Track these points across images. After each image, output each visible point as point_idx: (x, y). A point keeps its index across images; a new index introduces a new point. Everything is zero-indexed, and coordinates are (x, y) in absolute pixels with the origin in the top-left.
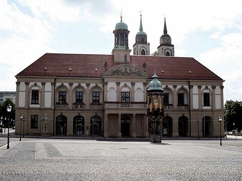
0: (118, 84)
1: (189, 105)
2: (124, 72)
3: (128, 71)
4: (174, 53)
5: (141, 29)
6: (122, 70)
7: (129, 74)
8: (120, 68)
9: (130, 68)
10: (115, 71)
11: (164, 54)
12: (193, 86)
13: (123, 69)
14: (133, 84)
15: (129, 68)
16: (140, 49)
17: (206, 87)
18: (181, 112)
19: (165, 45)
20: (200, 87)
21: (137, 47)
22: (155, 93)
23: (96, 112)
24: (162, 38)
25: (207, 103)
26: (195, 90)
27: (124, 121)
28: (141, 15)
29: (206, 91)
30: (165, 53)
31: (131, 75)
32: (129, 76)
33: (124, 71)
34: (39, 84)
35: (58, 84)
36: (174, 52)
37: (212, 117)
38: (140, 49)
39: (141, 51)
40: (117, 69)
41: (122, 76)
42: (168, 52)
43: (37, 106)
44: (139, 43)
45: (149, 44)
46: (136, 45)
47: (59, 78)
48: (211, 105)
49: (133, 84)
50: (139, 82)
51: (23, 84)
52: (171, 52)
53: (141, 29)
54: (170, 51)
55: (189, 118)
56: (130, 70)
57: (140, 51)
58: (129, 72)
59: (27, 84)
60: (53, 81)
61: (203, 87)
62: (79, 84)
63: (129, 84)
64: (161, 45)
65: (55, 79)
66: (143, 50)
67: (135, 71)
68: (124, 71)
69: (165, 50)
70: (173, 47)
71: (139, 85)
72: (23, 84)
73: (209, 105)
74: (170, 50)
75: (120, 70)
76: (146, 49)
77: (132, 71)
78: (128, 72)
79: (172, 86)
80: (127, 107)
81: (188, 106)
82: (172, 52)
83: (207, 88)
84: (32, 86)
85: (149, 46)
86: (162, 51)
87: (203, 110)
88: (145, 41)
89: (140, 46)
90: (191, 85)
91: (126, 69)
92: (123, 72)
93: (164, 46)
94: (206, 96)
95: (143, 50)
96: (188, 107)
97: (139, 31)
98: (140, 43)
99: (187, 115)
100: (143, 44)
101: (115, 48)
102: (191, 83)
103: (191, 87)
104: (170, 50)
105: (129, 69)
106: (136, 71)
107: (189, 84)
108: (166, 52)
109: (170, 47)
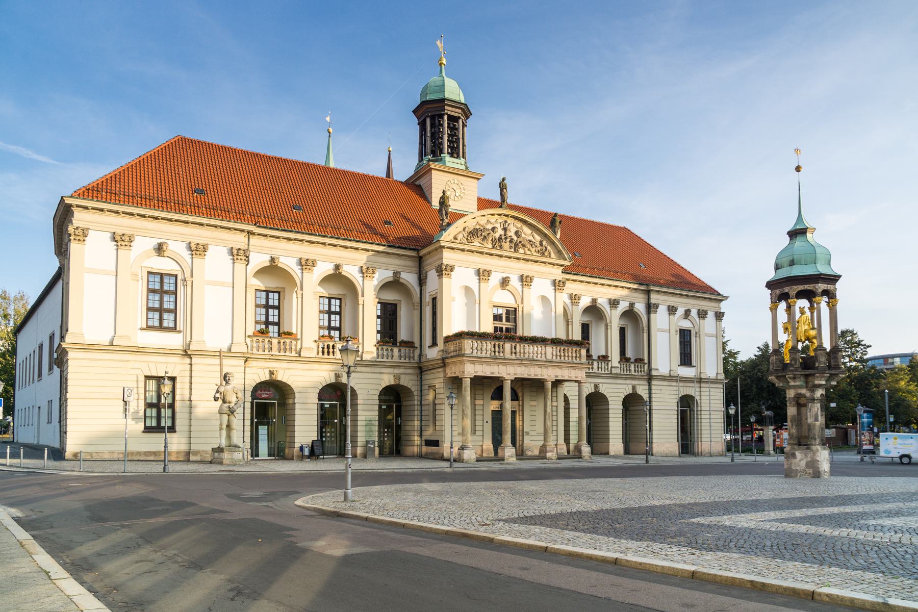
0: (484, 275)
1: (646, 361)
13: (498, 226)
18: (628, 382)
23: (397, 371)
31: (521, 251)
32: (516, 251)
33: (500, 232)
34: (177, 248)
37: (697, 398)
40: (482, 223)
43: (174, 341)
48: (694, 363)
49: (525, 280)
68: (500, 232)
71: (542, 286)
75: (489, 227)
92: (497, 235)
94: (685, 337)
99: (642, 391)
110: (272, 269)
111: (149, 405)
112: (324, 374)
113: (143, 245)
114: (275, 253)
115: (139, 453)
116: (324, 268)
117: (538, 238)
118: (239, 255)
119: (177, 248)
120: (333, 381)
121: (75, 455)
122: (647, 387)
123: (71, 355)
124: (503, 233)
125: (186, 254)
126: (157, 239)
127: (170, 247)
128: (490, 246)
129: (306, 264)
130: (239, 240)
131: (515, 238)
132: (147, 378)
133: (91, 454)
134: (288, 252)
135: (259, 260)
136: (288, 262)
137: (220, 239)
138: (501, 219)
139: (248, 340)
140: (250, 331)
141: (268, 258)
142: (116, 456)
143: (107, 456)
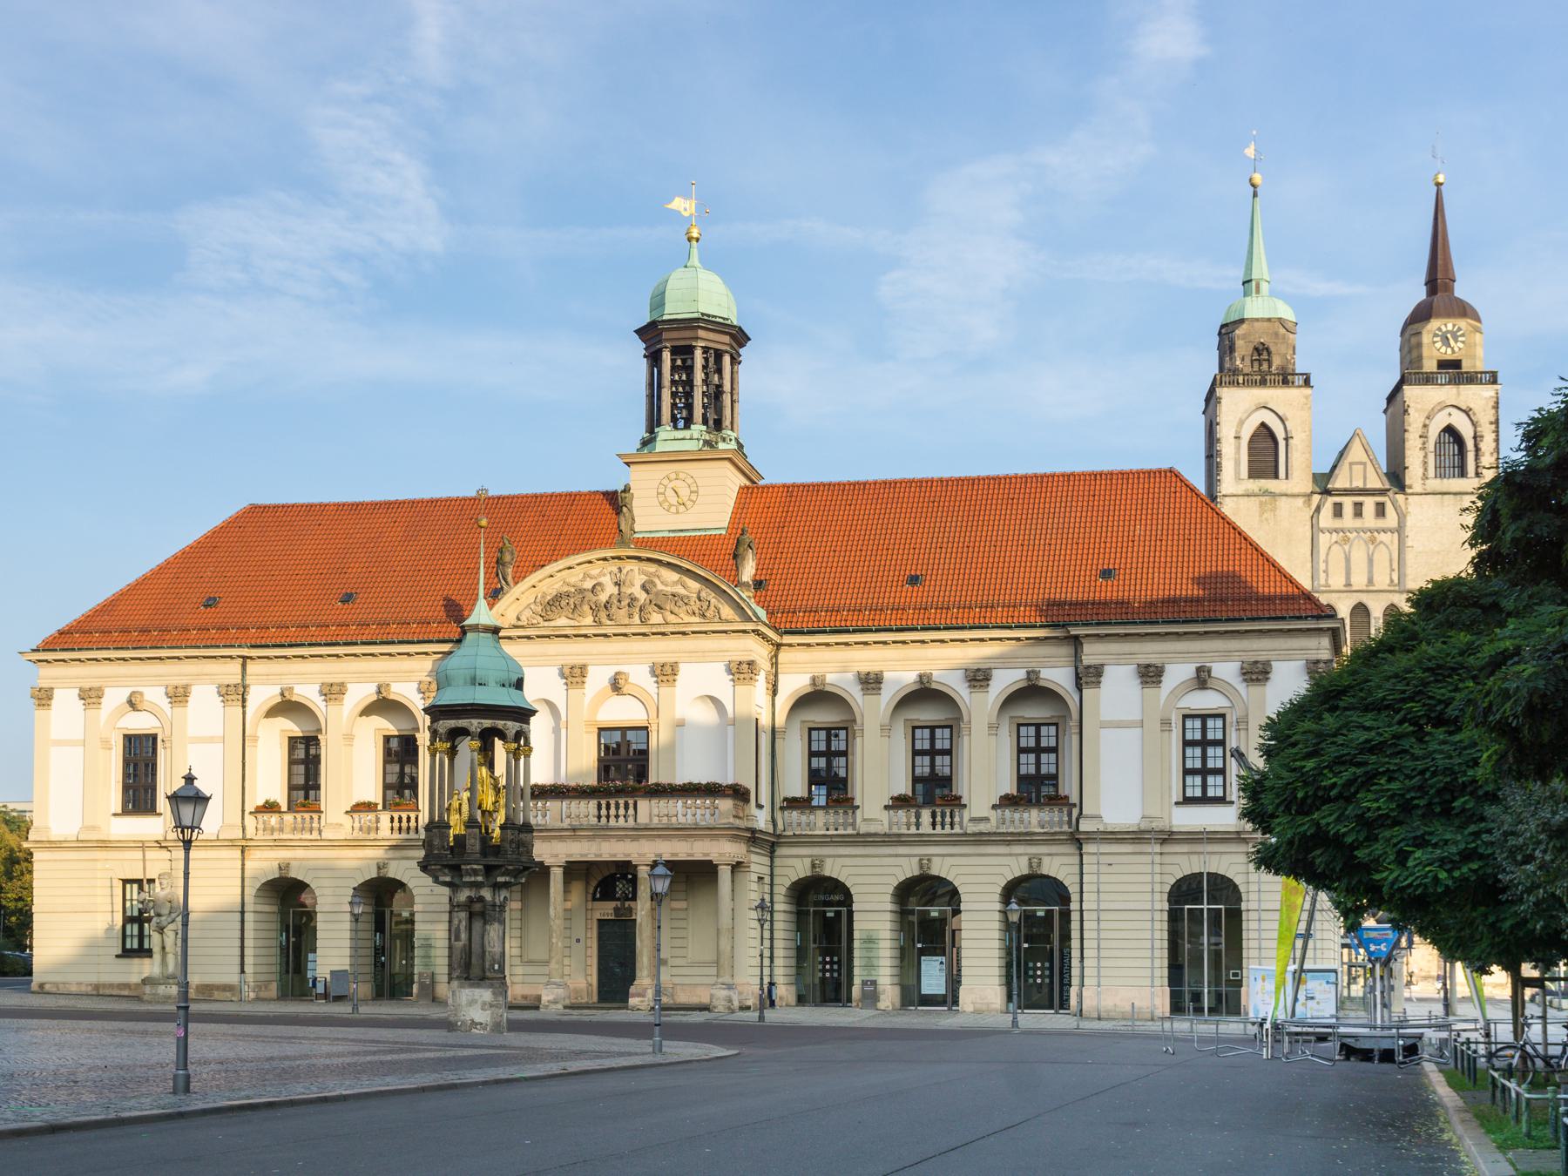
4: (1497, 432)
8: (586, 576)
10: (558, 598)
15: (642, 572)
16: (1241, 423)
17: (1199, 670)
27: (616, 909)
34: (155, 695)
38: (1241, 423)
39: (1246, 434)
40: (573, 580)
41: (599, 624)
42: (1450, 430)
47: (790, 645)
49: (665, 673)
50: (702, 657)
54: (1463, 415)
55: (1073, 890)
63: (639, 675)
66: (1263, 425)
72: (66, 700)
75: (588, 585)
83: (1202, 679)
87: (1168, 837)
92: (603, 598)
95: (1263, 425)
96: (1070, 815)
103: (1087, 677)
110: (287, 707)
111: (128, 920)
112: (361, 862)
113: (115, 697)
114: (287, 681)
115: (111, 986)
116: (361, 693)
117: (694, 585)
118: (237, 693)
119: (1226, 671)
120: (374, 875)
121: (41, 986)
122: (1076, 859)
123: (37, 856)
124: (615, 590)
125: (164, 703)
126: (135, 690)
127: (146, 697)
128: (589, 620)
129: (333, 692)
130: (230, 672)
131: (642, 597)
132: (125, 882)
133: (56, 984)
134: (304, 677)
135: (262, 695)
136: (308, 693)
137: (205, 677)
138: (613, 567)
139: (250, 820)
140: (249, 807)
141: (373, 688)
142: (83, 989)
143: (74, 989)
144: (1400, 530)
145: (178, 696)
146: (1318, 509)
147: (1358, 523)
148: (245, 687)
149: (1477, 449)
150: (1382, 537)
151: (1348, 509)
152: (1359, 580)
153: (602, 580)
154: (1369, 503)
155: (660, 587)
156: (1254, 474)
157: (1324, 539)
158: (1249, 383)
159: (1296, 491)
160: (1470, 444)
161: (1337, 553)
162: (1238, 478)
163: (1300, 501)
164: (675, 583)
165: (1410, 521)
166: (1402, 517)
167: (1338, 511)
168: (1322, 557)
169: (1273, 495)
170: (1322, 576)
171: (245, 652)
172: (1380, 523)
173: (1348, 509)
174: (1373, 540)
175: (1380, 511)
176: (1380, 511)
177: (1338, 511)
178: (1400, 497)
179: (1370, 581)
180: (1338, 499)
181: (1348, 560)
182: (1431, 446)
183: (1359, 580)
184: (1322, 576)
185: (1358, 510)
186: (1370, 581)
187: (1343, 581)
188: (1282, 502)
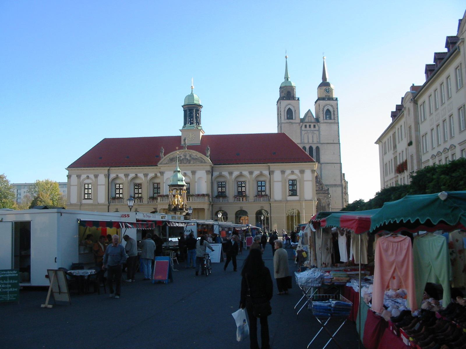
2: (183, 159)
3: (188, 157)
4: (338, 110)
5: (287, 78)
6: (180, 156)
7: (189, 161)
9: (190, 153)
11: (322, 112)
12: (273, 172)
14: (194, 173)
16: (285, 107)
19: (323, 99)
20: (283, 172)
21: (280, 106)
22: (174, 188)
24: (319, 89)
25: (293, 193)
26: (277, 176)
28: (286, 58)
29: (293, 177)
30: (323, 111)
32: (189, 163)
35: (112, 176)
36: (337, 108)
38: (285, 107)
44: (284, 100)
45: (298, 99)
46: (279, 103)
49: (194, 173)
51: (74, 178)
52: (334, 108)
53: (287, 78)
54: (331, 107)
56: (190, 156)
57: (284, 111)
58: (189, 158)
59: (79, 176)
60: (106, 172)
61: (288, 172)
62: (136, 175)
64: (319, 99)
65: (109, 169)
67: (197, 158)
68: (183, 157)
69: (324, 107)
70: (336, 102)
73: (296, 195)
74: (332, 106)
76: (294, 107)
77: (192, 157)
78: (187, 159)
79: (247, 172)
80: (162, 201)
81: (268, 197)
82: (336, 110)
83: (293, 173)
84: (84, 179)
85: (299, 103)
86: (319, 108)
88: (292, 95)
89: (285, 103)
90: (271, 169)
91: (185, 156)
92: (181, 159)
93: (321, 101)
96: (268, 198)
97: (283, 80)
98: (285, 98)
100: (289, 99)
101: (183, 127)
102: (271, 167)
104: (332, 106)
105: (189, 155)
106: (197, 157)
107: (269, 168)
108: (325, 110)
109: (331, 102)
144: (319, 130)
145: (96, 176)
146: (302, 126)
147: (310, 129)
148: (109, 175)
149: (334, 114)
150: (315, 132)
151: (308, 126)
152: (310, 141)
153: (181, 155)
154: (312, 125)
155: (192, 157)
156: (288, 118)
157: (303, 132)
158: (287, 100)
159: (297, 122)
160: (332, 113)
161: (306, 136)
162: (285, 119)
163: (298, 124)
164: (195, 156)
165: (321, 129)
166: (319, 127)
167: (306, 126)
168: (303, 136)
169: (292, 123)
170: (303, 140)
171: (108, 168)
172: (315, 129)
173: (308, 126)
174: (313, 133)
175: (314, 126)
176: (314, 126)
177: (306, 126)
178: (318, 123)
179: (313, 141)
180: (306, 124)
181: (308, 137)
182: (325, 112)
183: (310, 141)
184: (303, 140)
185: (310, 126)
186: (313, 141)
187: (307, 141)
188: (294, 125)
